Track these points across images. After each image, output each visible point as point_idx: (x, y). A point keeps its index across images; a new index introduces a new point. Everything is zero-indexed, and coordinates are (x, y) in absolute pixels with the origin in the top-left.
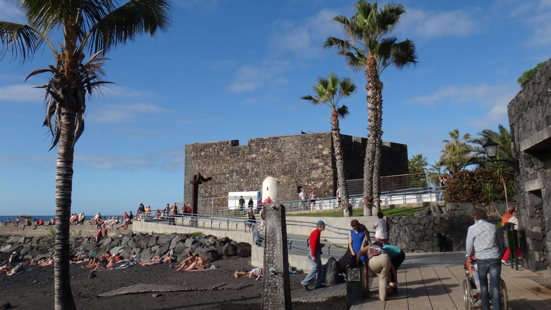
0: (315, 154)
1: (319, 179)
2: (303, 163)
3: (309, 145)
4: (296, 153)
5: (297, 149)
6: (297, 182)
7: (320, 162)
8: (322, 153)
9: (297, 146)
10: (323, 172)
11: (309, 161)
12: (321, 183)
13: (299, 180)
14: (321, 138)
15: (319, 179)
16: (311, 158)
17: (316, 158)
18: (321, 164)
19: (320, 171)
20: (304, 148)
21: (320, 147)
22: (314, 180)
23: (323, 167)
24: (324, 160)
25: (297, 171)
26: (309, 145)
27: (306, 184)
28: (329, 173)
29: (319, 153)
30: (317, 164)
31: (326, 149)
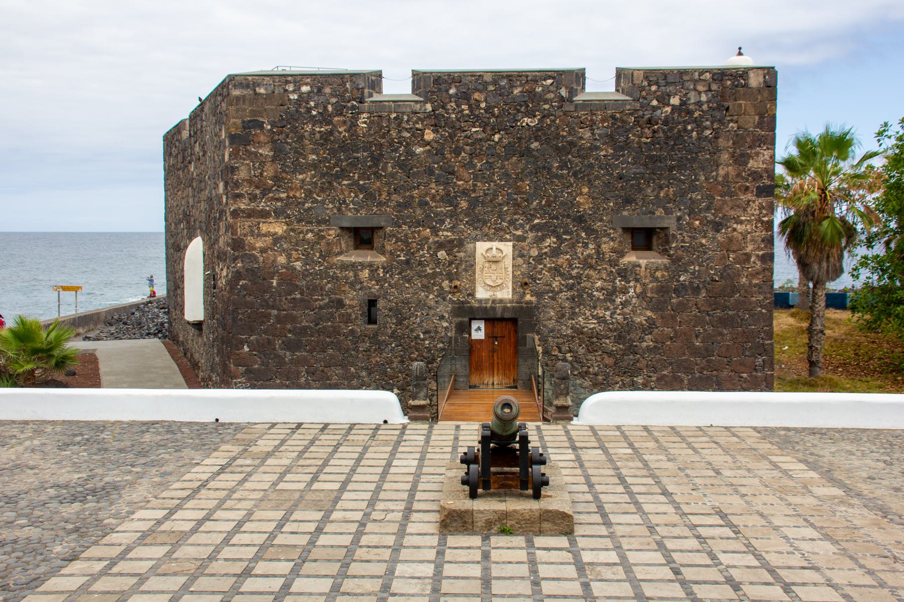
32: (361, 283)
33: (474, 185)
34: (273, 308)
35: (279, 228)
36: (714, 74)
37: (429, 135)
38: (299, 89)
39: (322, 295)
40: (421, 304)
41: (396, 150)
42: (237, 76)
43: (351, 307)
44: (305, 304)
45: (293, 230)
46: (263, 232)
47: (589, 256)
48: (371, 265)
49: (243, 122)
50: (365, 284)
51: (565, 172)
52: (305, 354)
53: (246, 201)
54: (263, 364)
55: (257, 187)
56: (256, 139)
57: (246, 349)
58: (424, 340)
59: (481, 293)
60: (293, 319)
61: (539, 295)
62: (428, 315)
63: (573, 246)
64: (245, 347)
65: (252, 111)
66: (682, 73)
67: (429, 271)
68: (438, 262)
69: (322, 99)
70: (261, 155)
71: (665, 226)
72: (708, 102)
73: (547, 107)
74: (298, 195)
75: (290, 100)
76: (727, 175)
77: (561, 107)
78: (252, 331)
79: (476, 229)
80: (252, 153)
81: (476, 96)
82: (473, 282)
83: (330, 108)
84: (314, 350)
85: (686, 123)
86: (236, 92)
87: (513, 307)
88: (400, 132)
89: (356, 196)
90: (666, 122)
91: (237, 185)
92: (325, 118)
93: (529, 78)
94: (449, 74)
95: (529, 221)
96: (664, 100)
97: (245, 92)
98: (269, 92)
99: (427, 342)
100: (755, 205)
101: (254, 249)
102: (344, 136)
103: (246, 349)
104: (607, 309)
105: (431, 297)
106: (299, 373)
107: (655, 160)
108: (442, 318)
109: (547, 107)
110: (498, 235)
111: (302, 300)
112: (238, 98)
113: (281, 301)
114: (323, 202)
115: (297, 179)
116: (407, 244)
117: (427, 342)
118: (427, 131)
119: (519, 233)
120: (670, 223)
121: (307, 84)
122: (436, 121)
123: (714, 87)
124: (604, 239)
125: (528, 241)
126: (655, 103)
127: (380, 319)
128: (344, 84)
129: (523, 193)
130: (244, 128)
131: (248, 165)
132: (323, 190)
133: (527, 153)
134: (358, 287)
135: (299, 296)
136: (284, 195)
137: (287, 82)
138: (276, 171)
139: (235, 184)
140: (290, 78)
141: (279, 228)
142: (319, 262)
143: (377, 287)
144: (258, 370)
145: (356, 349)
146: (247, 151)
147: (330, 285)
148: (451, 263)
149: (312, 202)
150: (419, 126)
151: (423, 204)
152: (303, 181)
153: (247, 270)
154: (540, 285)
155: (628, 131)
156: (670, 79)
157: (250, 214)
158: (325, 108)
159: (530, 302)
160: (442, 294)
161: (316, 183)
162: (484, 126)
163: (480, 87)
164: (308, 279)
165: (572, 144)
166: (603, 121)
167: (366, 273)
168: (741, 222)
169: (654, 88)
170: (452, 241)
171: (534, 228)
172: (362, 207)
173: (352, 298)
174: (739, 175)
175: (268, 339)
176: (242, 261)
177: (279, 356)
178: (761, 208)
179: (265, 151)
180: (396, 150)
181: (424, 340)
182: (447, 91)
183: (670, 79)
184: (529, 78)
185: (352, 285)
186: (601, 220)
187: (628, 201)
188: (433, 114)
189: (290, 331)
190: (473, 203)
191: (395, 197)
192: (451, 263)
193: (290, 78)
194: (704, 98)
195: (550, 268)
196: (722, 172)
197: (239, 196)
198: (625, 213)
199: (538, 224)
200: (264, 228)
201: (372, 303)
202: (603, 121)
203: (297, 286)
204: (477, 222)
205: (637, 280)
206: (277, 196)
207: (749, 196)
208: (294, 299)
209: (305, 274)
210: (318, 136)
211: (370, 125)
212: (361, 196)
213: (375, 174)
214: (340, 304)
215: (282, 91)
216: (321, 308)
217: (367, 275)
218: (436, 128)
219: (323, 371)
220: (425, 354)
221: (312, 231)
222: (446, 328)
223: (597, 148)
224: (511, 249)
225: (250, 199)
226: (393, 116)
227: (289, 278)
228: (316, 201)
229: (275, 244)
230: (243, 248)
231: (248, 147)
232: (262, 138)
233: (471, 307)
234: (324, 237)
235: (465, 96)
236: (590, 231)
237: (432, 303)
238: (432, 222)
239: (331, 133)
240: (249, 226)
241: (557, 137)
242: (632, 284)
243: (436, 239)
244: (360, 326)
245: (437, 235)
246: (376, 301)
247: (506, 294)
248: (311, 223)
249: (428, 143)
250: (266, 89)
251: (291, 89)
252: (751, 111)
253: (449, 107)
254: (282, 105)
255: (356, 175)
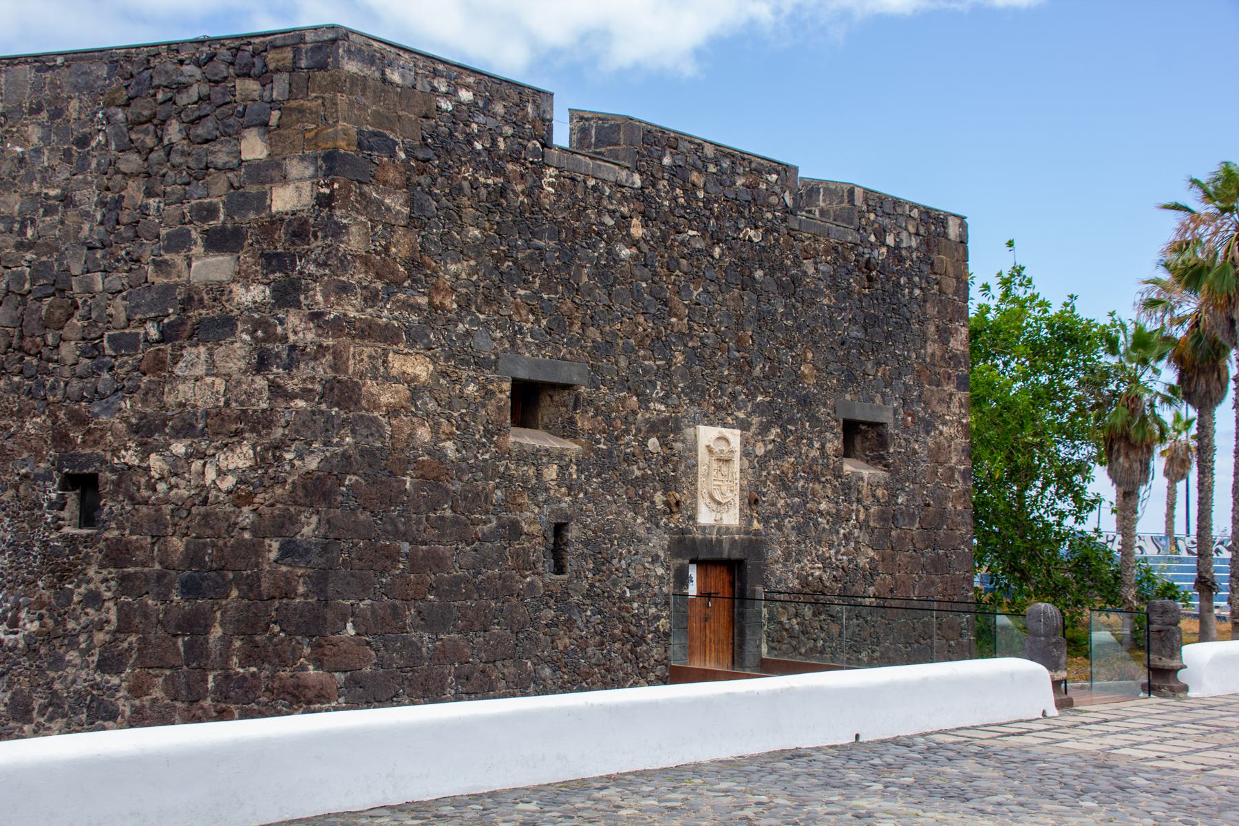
0: (211, 212)
1: (224, 425)
2: (118, 279)
3: (174, 132)
4: (66, 200)
5: (83, 167)
6: (61, 438)
7: (243, 277)
8: (261, 201)
9: (83, 141)
10: (262, 364)
11: (161, 266)
12: (240, 458)
13: (79, 420)
14: (265, 77)
15: (224, 425)
16: (179, 242)
17: (219, 241)
18: (252, 294)
19: (236, 353)
20: (132, 162)
21: (254, 148)
22: (186, 430)
23: (263, 326)
24: (272, 261)
25: (68, 351)
26: (174, 132)
27: (130, 457)
28: (304, 370)
29: (239, 201)
30: (220, 291)
31: (296, 168)
32: (547, 490)
33: (691, 328)
34: (405, 537)
35: (421, 369)
36: (921, 213)
37: (637, 231)
38: (456, 91)
39: (487, 512)
40: (631, 538)
41: (594, 246)
42: (353, 32)
43: (531, 536)
44: (461, 530)
45: (444, 374)
46: (394, 372)
47: (814, 459)
48: (561, 456)
49: (360, 132)
50: (552, 492)
51: (790, 323)
52: (455, 636)
53: (357, 301)
54: (380, 664)
55: (379, 276)
56: (380, 174)
57: (350, 630)
58: (631, 600)
59: (705, 517)
60: (437, 561)
61: (765, 520)
62: (636, 554)
63: (798, 442)
64: (349, 625)
65: (376, 113)
66: (897, 202)
67: (638, 473)
68: (647, 456)
69: (491, 123)
70: (388, 209)
71: (878, 420)
72: (917, 249)
73: (769, 216)
74: (447, 302)
75: (439, 108)
76: (933, 354)
77: (784, 220)
78: (365, 589)
79: (692, 402)
80: (371, 201)
81: (694, 177)
82: (694, 495)
83: (502, 145)
84: (470, 627)
85: (900, 274)
86: (351, 67)
87: (742, 540)
88: (599, 214)
89: (537, 321)
90: (883, 269)
91: (344, 264)
92: (493, 161)
93: (753, 165)
94: (663, 131)
95: (751, 396)
96: (881, 233)
97: (367, 72)
98: (409, 83)
99: (635, 605)
100: (955, 400)
101: (377, 407)
102: (522, 202)
103: (350, 630)
104: (831, 546)
105: (639, 521)
106: (443, 678)
107: (874, 321)
108: (655, 559)
109: (769, 216)
110: (718, 416)
111: (455, 522)
112: (354, 79)
113: (419, 522)
114: (486, 324)
115: (446, 271)
116: (608, 418)
117: (635, 605)
118: (635, 221)
119: (741, 415)
120: (886, 417)
121: (468, 87)
122: (645, 203)
123: (922, 231)
124: (829, 435)
125: (753, 429)
126: (872, 238)
127: (571, 562)
128: (521, 105)
129: (745, 350)
130: (360, 145)
131: (364, 224)
132: (488, 301)
133: (748, 283)
134: (541, 498)
135: (449, 513)
136: (423, 301)
137: (436, 73)
138: (413, 249)
139: (342, 262)
140: (441, 67)
141: (421, 369)
142: (484, 445)
143: (568, 499)
144: (373, 677)
145: (534, 621)
146: (362, 194)
147: (499, 493)
148: (666, 460)
149: (471, 322)
150: (625, 210)
151: (628, 350)
152: (457, 276)
153: (363, 452)
154: (765, 508)
155: (849, 273)
156: (888, 208)
157: (367, 331)
158: (494, 142)
159: (757, 533)
160: (653, 518)
161: (476, 285)
162: (704, 230)
163: (699, 163)
164: (466, 478)
165: (795, 281)
166: (826, 252)
167: (551, 472)
168: (945, 423)
169: (872, 216)
170: (665, 421)
171: (759, 409)
172: (546, 344)
173: (533, 520)
174: (942, 357)
175: (394, 608)
176: (353, 432)
177: (412, 644)
178: (961, 406)
179: (396, 203)
180: (594, 246)
181: (631, 600)
182: (660, 159)
183: (888, 208)
184: (753, 165)
185: (534, 492)
186: (825, 405)
187: (851, 378)
188: (640, 194)
189: (431, 589)
190: (693, 356)
191: (593, 332)
192: (666, 460)
193: (441, 67)
194: (914, 244)
195: (775, 476)
196: (929, 350)
197: (345, 289)
198: (848, 397)
199: (762, 403)
200: (397, 364)
201: (559, 529)
202: (826, 252)
203: (447, 491)
204: (696, 391)
205: (859, 501)
206: (412, 301)
207: (950, 388)
208: (442, 518)
209: (459, 469)
210: (483, 192)
211: (559, 187)
212: (544, 322)
213: (566, 283)
214: (514, 530)
215: (428, 89)
216: (485, 539)
217: (554, 476)
218: (646, 219)
219: (483, 672)
220: (633, 628)
221: (474, 379)
222: (661, 578)
223: (821, 293)
224: (738, 439)
225: (365, 300)
226: (591, 182)
227: (435, 474)
228: (479, 323)
229: (413, 398)
230: (357, 402)
231: (366, 189)
232: (392, 175)
233: (694, 540)
234: (493, 393)
235: (678, 173)
236: (814, 420)
237: (641, 532)
238: (636, 385)
239: (503, 192)
240: (370, 357)
241: (782, 267)
242: (854, 507)
243: (648, 416)
244: (544, 578)
245: (648, 409)
246: (566, 524)
247: (732, 518)
248: (468, 363)
249: (634, 243)
250: (403, 76)
251: (443, 89)
252: (950, 270)
253: (661, 187)
254: (426, 117)
255: (538, 281)
